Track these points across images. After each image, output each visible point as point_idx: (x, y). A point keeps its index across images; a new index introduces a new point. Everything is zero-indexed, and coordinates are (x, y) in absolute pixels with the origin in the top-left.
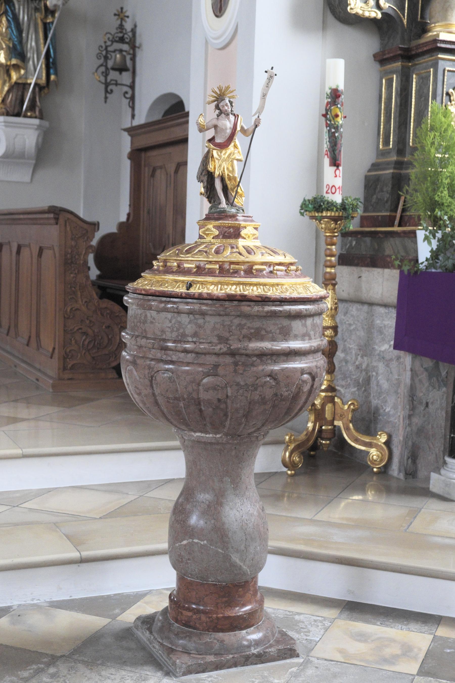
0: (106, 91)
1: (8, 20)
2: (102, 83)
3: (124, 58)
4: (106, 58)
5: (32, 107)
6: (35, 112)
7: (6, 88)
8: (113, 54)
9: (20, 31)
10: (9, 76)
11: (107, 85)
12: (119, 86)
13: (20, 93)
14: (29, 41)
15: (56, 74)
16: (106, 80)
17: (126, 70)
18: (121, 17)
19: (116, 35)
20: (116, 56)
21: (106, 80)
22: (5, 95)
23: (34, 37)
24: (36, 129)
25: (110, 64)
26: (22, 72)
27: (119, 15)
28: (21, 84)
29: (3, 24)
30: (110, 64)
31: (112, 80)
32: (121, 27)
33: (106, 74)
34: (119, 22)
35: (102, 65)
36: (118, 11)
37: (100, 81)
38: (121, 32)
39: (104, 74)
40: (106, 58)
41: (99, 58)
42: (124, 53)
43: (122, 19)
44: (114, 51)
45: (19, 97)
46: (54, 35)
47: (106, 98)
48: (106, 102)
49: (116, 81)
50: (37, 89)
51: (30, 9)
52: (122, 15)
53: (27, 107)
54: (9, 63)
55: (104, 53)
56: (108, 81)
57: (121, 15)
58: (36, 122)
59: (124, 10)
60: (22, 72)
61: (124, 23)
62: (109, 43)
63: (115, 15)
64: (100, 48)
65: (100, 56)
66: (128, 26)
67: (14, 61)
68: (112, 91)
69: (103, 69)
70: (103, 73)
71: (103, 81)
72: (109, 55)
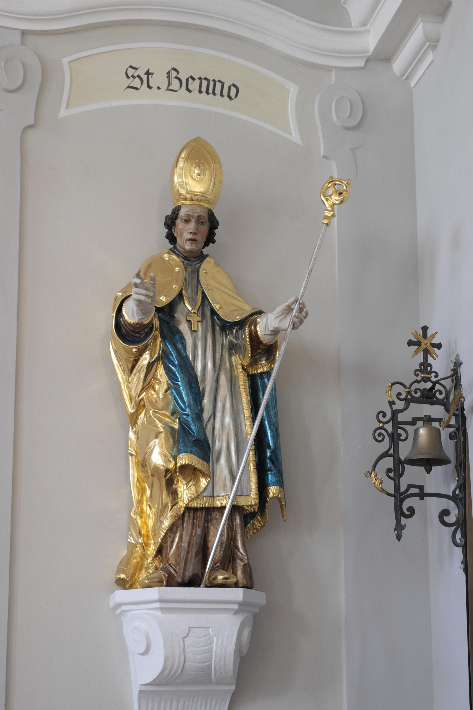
0: (400, 513)
1: (169, 372)
3: (435, 436)
4: (395, 439)
5: (228, 559)
6: (235, 573)
7: (167, 523)
9: (197, 395)
10: (174, 494)
11: (399, 497)
12: (427, 499)
13: (199, 531)
14: (219, 415)
15: (280, 483)
16: (397, 486)
17: (442, 461)
18: (423, 347)
19: (415, 386)
20: (416, 431)
22: (165, 537)
23: (228, 405)
24: (236, 612)
25: (405, 450)
26: (203, 482)
27: (418, 343)
28: (202, 509)
29: (160, 382)
30: (405, 450)
31: (410, 486)
32: (425, 367)
33: (396, 474)
34: (420, 358)
35: (385, 455)
36: (417, 335)
37: (382, 490)
38: (426, 380)
39: (392, 475)
40: (395, 439)
41: (381, 438)
42: (436, 424)
43: (426, 352)
44: (414, 421)
45: (196, 541)
46: (273, 398)
47: (399, 528)
48: (399, 537)
49: (421, 487)
50: (238, 520)
51: (219, 347)
52: (425, 344)
53: (214, 562)
54: (171, 466)
55: (389, 427)
56: (403, 489)
57: (423, 342)
58: (237, 594)
59: (429, 333)
60: (203, 482)
61: (430, 360)
62: (400, 405)
63: (410, 343)
64: (381, 414)
65: (380, 435)
66: (440, 365)
67: (184, 459)
68: (412, 511)
69: (389, 462)
70: (389, 470)
71: (392, 492)
72: (400, 431)
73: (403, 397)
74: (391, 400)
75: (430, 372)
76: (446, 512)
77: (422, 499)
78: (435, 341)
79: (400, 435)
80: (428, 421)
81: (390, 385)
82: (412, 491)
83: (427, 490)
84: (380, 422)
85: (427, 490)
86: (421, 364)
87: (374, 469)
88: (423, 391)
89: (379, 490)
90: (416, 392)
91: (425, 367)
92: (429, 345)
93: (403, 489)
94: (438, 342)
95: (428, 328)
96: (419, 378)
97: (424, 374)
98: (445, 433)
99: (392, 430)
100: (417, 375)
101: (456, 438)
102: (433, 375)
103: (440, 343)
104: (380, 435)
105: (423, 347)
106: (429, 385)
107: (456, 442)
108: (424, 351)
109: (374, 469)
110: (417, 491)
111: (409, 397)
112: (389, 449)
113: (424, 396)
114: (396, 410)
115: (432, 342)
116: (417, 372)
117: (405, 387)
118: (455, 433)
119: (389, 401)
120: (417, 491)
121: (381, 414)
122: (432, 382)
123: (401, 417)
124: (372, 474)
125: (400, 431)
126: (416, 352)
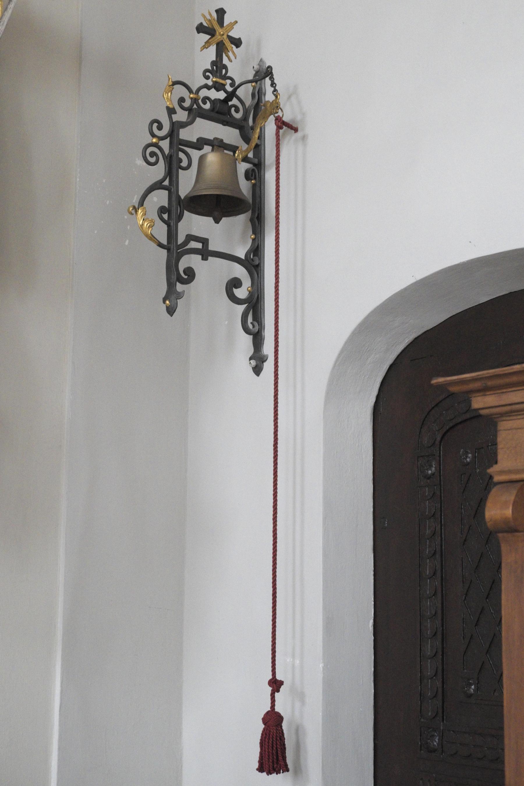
2: (160, 245)
4: (173, 166)
8: (195, 154)
11: (174, 249)
16: (172, 234)
18: (218, 38)
19: (204, 93)
20: (202, 159)
21: (172, 234)
25: (187, 183)
30: (187, 183)
31: (190, 238)
32: (218, 68)
33: (171, 215)
34: (211, 53)
37: (152, 238)
38: (218, 87)
39: (165, 216)
40: (173, 166)
41: (153, 160)
43: (221, 49)
49: (205, 242)
55: (165, 145)
56: (181, 239)
59: (227, 20)
61: (225, 61)
62: (181, 116)
63: (201, 29)
64: (155, 125)
65: (153, 154)
66: (239, 68)
70: (162, 210)
71: (164, 242)
72: (181, 155)
73: (187, 104)
74: (171, 106)
75: (225, 77)
76: (235, 283)
77: (205, 258)
78: (234, 34)
79: (181, 161)
80: (220, 146)
81: (171, 83)
82: (194, 245)
83: (212, 247)
84: (153, 135)
85: (211, 248)
86: (213, 63)
87: (141, 203)
88: (214, 102)
89: (147, 236)
90: (205, 103)
91: (218, 68)
92: (225, 36)
93: (181, 239)
94: (237, 37)
95: (225, 12)
96: (210, 83)
97: (216, 77)
98: (243, 167)
99: (171, 150)
100: (207, 78)
101: (255, 179)
102: (229, 82)
103: (240, 39)
104: (153, 154)
105: (218, 38)
106: (222, 95)
107: (254, 186)
108: (218, 45)
109: (141, 203)
110: (199, 246)
111: (195, 106)
112: (164, 180)
113: (216, 110)
114: (177, 122)
115: (229, 34)
116: (208, 74)
117: (190, 91)
118: (253, 170)
119: (168, 108)
120: (199, 246)
121: (155, 125)
122: (226, 91)
123: (184, 134)
124: (140, 211)
125: (181, 155)
126: (207, 45)
